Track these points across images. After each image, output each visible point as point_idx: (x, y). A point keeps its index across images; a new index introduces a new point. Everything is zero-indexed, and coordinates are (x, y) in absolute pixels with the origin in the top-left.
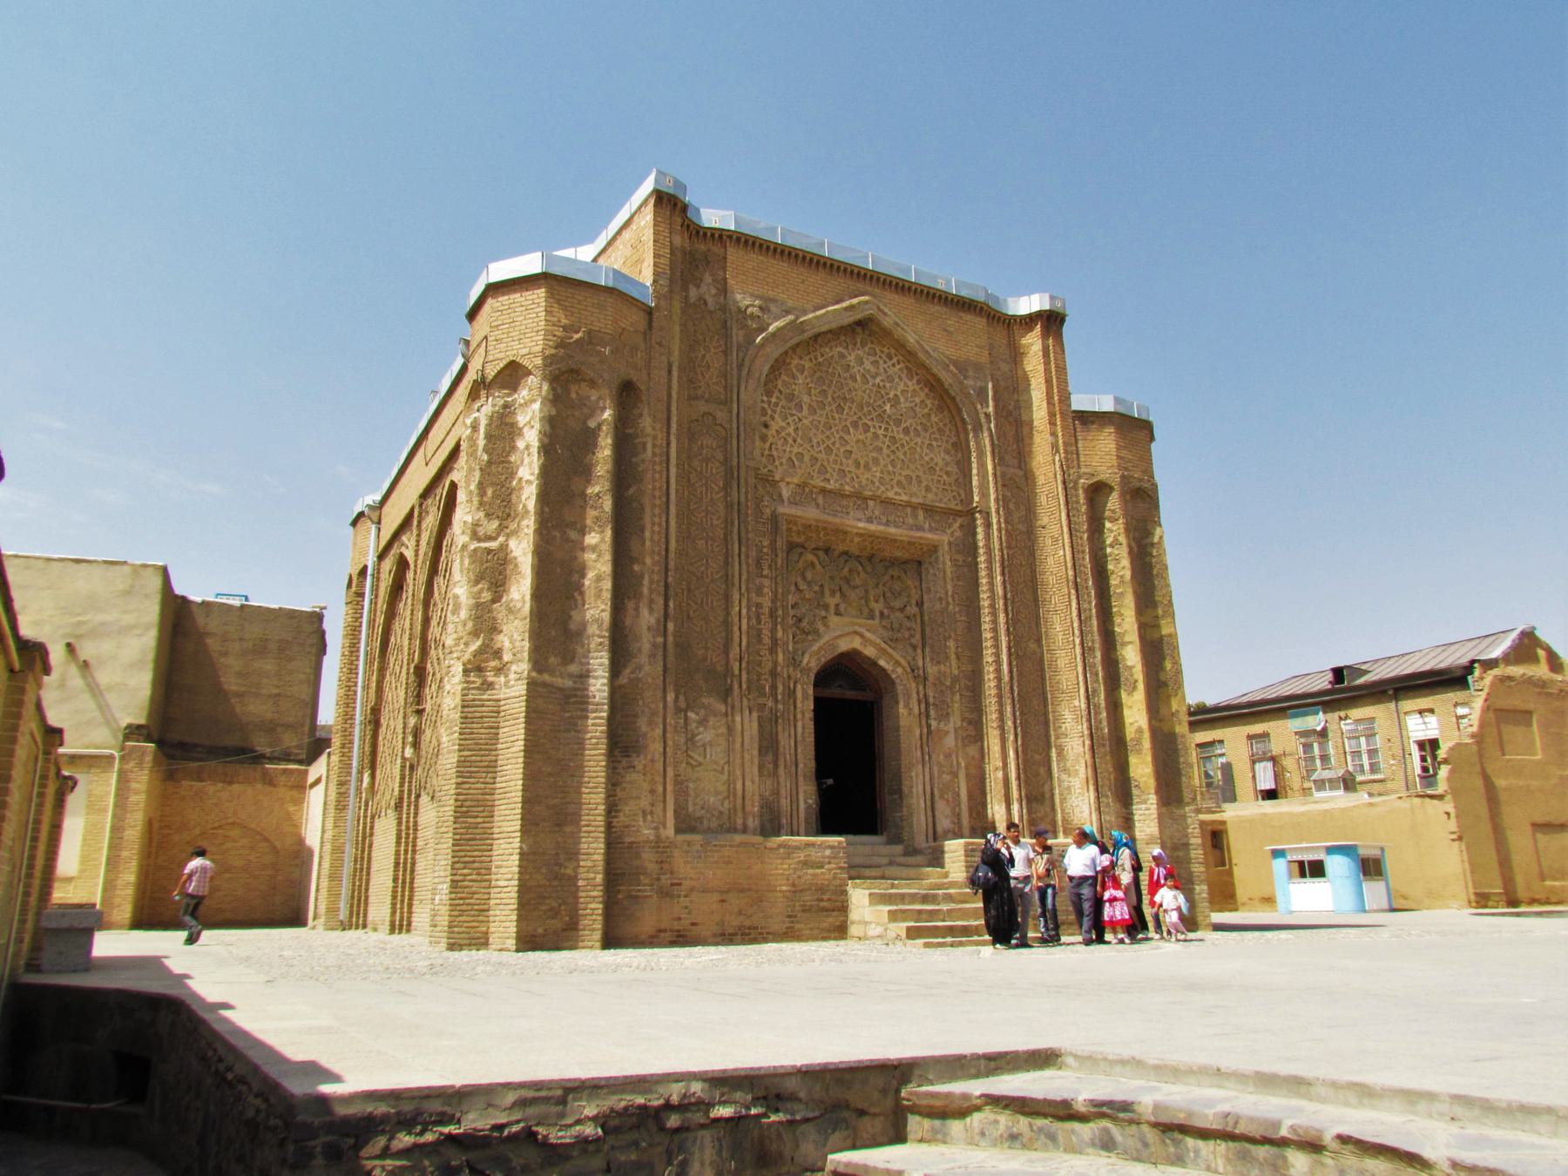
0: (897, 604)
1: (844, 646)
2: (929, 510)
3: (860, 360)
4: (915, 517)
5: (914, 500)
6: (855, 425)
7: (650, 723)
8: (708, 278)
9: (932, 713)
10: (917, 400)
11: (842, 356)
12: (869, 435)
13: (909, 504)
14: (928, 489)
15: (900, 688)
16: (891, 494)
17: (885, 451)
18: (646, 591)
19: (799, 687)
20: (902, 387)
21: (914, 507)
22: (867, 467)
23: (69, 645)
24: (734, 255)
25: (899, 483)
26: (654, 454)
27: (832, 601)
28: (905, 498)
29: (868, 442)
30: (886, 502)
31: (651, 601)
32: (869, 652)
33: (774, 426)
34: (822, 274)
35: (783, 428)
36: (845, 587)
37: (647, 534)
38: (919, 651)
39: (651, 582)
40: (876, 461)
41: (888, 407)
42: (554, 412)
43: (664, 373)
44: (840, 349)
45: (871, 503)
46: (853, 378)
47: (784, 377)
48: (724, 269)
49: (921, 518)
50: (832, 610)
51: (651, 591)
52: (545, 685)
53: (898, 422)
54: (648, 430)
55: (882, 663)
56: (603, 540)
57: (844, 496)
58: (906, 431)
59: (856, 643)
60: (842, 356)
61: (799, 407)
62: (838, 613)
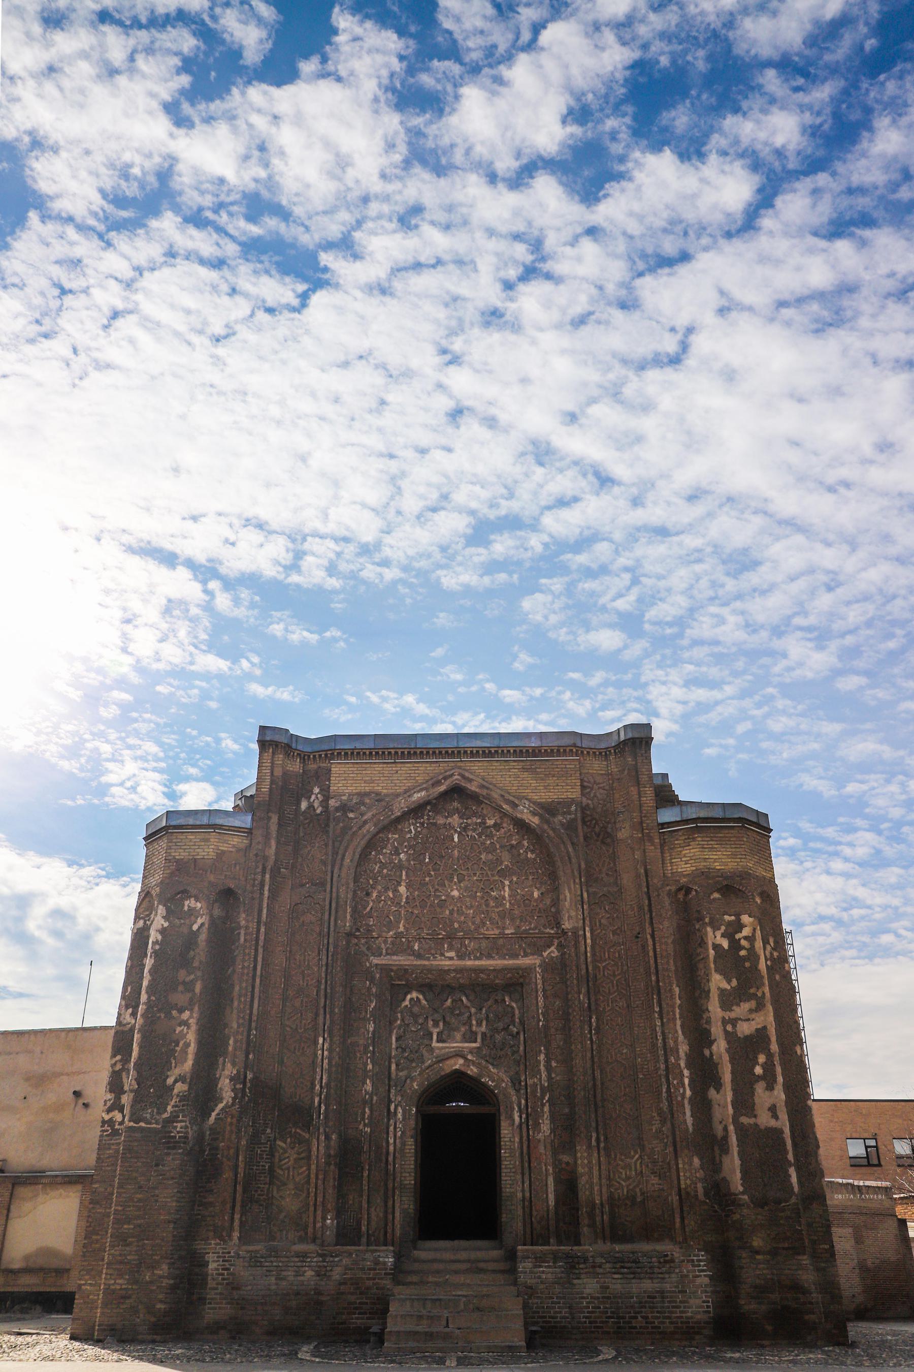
0: (500, 1025)
8: (316, 790)
9: (530, 1123)
18: (230, 1048)
19: (400, 1110)
23: (75, 1093)
24: (338, 768)
26: (245, 940)
31: (235, 1056)
32: (473, 1071)
37: (236, 1003)
38: (522, 1067)
39: (236, 1042)
42: (166, 924)
48: (329, 780)
50: (435, 1037)
51: (235, 1049)
52: (142, 1129)
54: (243, 923)
56: (191, 1017)
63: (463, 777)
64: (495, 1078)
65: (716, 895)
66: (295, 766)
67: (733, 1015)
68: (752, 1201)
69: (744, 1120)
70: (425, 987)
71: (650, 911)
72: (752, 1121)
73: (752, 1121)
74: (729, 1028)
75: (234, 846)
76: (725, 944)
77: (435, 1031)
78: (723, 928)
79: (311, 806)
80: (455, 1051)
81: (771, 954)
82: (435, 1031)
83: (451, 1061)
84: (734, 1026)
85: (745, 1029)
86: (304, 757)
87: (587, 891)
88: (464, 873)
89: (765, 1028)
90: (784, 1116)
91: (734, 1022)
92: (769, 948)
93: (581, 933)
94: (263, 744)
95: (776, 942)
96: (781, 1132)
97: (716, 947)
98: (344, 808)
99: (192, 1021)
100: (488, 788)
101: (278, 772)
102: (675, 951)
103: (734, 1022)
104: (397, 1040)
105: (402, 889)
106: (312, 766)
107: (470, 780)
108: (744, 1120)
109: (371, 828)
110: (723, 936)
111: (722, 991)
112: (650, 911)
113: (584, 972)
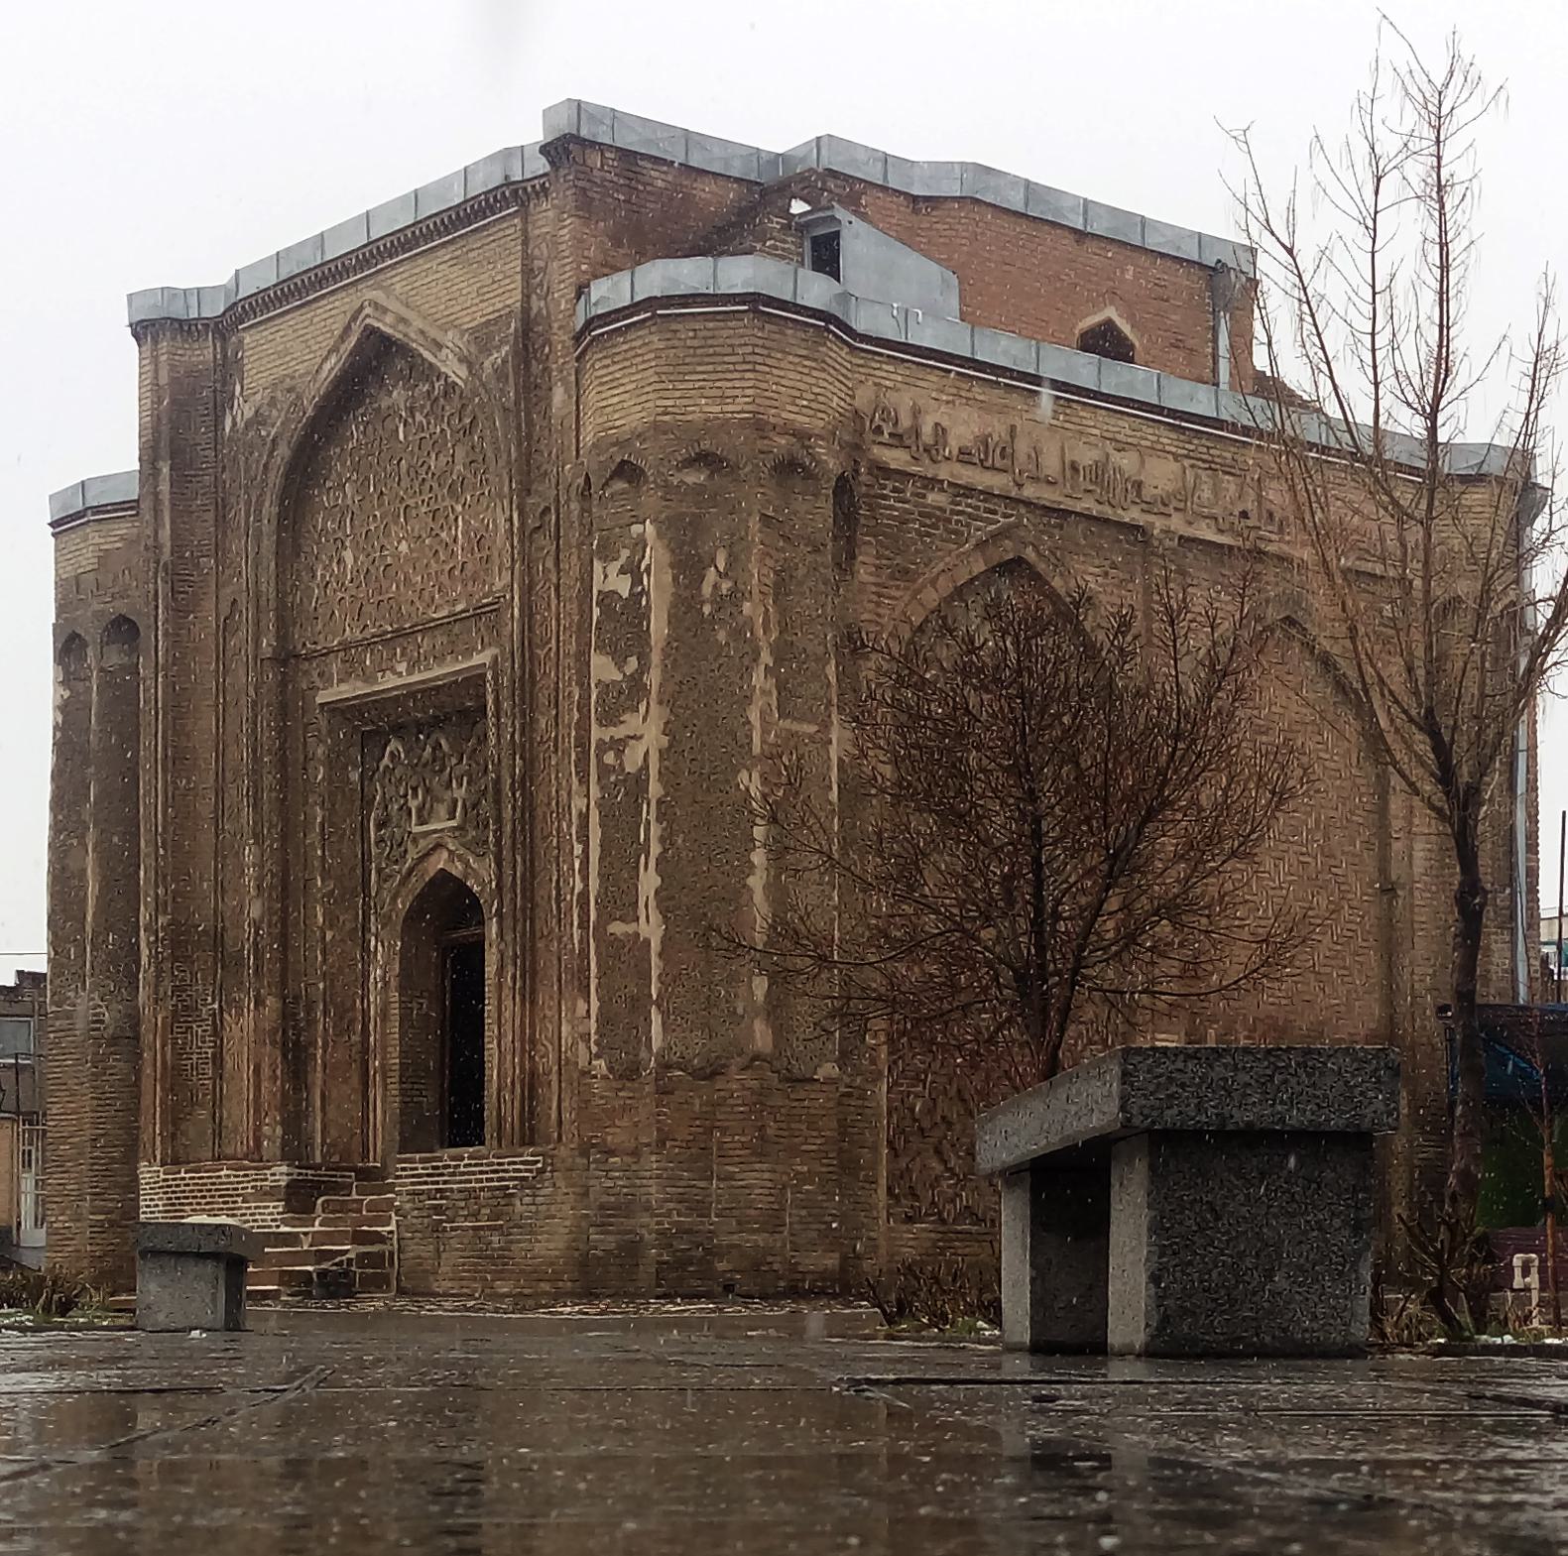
32: (457, 869)
62: (422, 822)
66: (205, 352)
67: (619, 732)
68: (611, 1069)
69: (617, 928)
70: (398, 730)
72: (630, 928)
73: (630, 928)
74: (609, 758)
76: (623, 586)
77: (413, 804)
78: (625, 553)
80: (438, 838)
81: (716, 587)
82: (413, 804)
83: (433, 859)
84: (620, 753)
85: (632, 760)
88: (411, 502)
90: (655, 916)
91: (619, 746)
92: (711, 575)
94: (143, 330)
95: (730, 564)
96: (647, 942)
97: (607, 597)
101: (164, 379)
103: (619, 746)
104: (380, 826)
105: (348, 556)
108: (617, 928)
109: (283, 451)
110: (622, 571)
111: (605, 687)
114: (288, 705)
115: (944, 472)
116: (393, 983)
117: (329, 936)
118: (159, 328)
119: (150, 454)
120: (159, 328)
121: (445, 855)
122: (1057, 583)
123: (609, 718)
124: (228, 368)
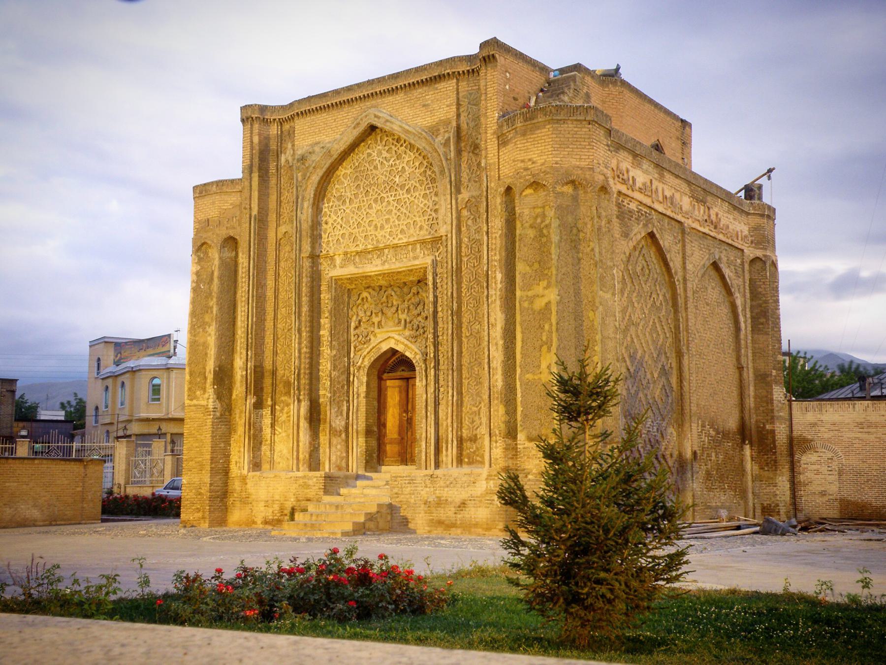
1: (385, 347)
2: (423, 242)
3: (375, 152)
4: (414, 250)
5: (412, 240)
6: (376, 201)
7: (240, 417)
10: (417, 164)
11: (369, 155)
12: (384, 204)
13: (408, 244)
14: (421, 228)
15: (417, 369)
16: (396, 241)
17: (394, 211)
18: (238, 348)
20: (407, 159)
21: (414, 244)
22: (382, 227)
24: (300, 125)
25: (402, 231)
27: (376, 320)
28: (405, 240)
29: (383, 210)
30: (395, 247)
32: (400, 348)
33: (331, 221)
34: (346, 108)
35: (335, 221)
36: (384, 309)
40: (387, 221)
41: (397, 179)
43: (248, 225)
44: (369, 151)
45: (386, 251)
46: (376, 168)
47: (337, 186)
49: (418, 250)
52: (195, 406)
53: (402, 187)
55: (408, 354)
57: (369, 252)
58: (408, 191)
59: (392, 344)
60: (369, 155)
61: (344, 201)
63: (376, 116)
64: (412, 352)
65: (529, 191)
67: (530, 293)
69: (529, 376)
71: (487, 211)
74: (526, 304)
75: (231, 204)
79: (287, 161)
85: (539, 304)
86: (281, 122)
87: (457, 200)
88: (385, 195)
89: (550, 302)
93: (449, 235)
98: (303, 159)
99: (213, 333)
100: (391, 122)
101: (256, 139)
102: (501, 243)
103: (531, 300)
106: (286, 127)
107: (379, 117)
108: (529, 376)
112: (487, 211)
113: (450, 267)
114: (316, 277)
115: (637, 195)
116: (363, 395)
117: (334, 373)
118: (254, 116)
119: (249, 169)
120: (254, 116)
121: (393, 341)
122: (661, 242)
123: (527, 287)
124: (287, 136)
